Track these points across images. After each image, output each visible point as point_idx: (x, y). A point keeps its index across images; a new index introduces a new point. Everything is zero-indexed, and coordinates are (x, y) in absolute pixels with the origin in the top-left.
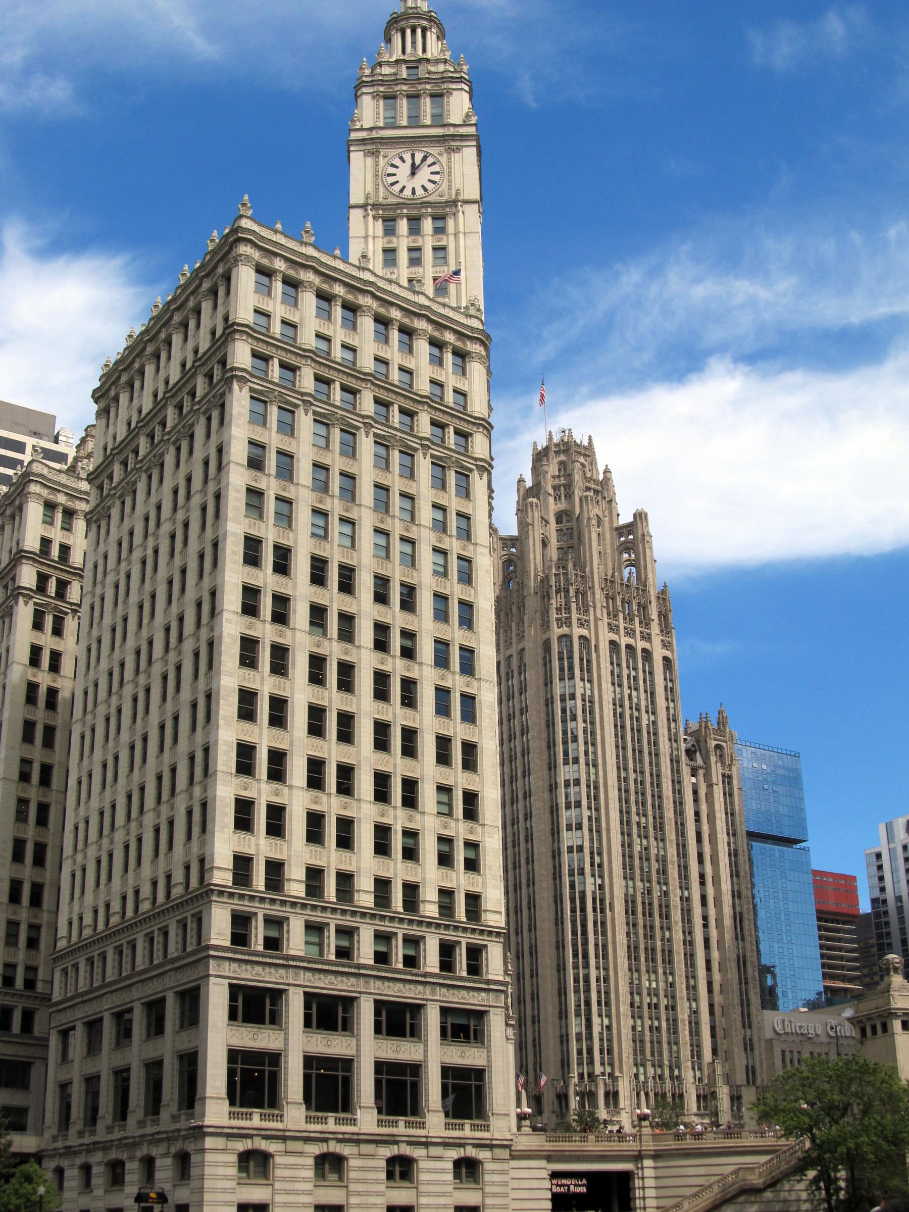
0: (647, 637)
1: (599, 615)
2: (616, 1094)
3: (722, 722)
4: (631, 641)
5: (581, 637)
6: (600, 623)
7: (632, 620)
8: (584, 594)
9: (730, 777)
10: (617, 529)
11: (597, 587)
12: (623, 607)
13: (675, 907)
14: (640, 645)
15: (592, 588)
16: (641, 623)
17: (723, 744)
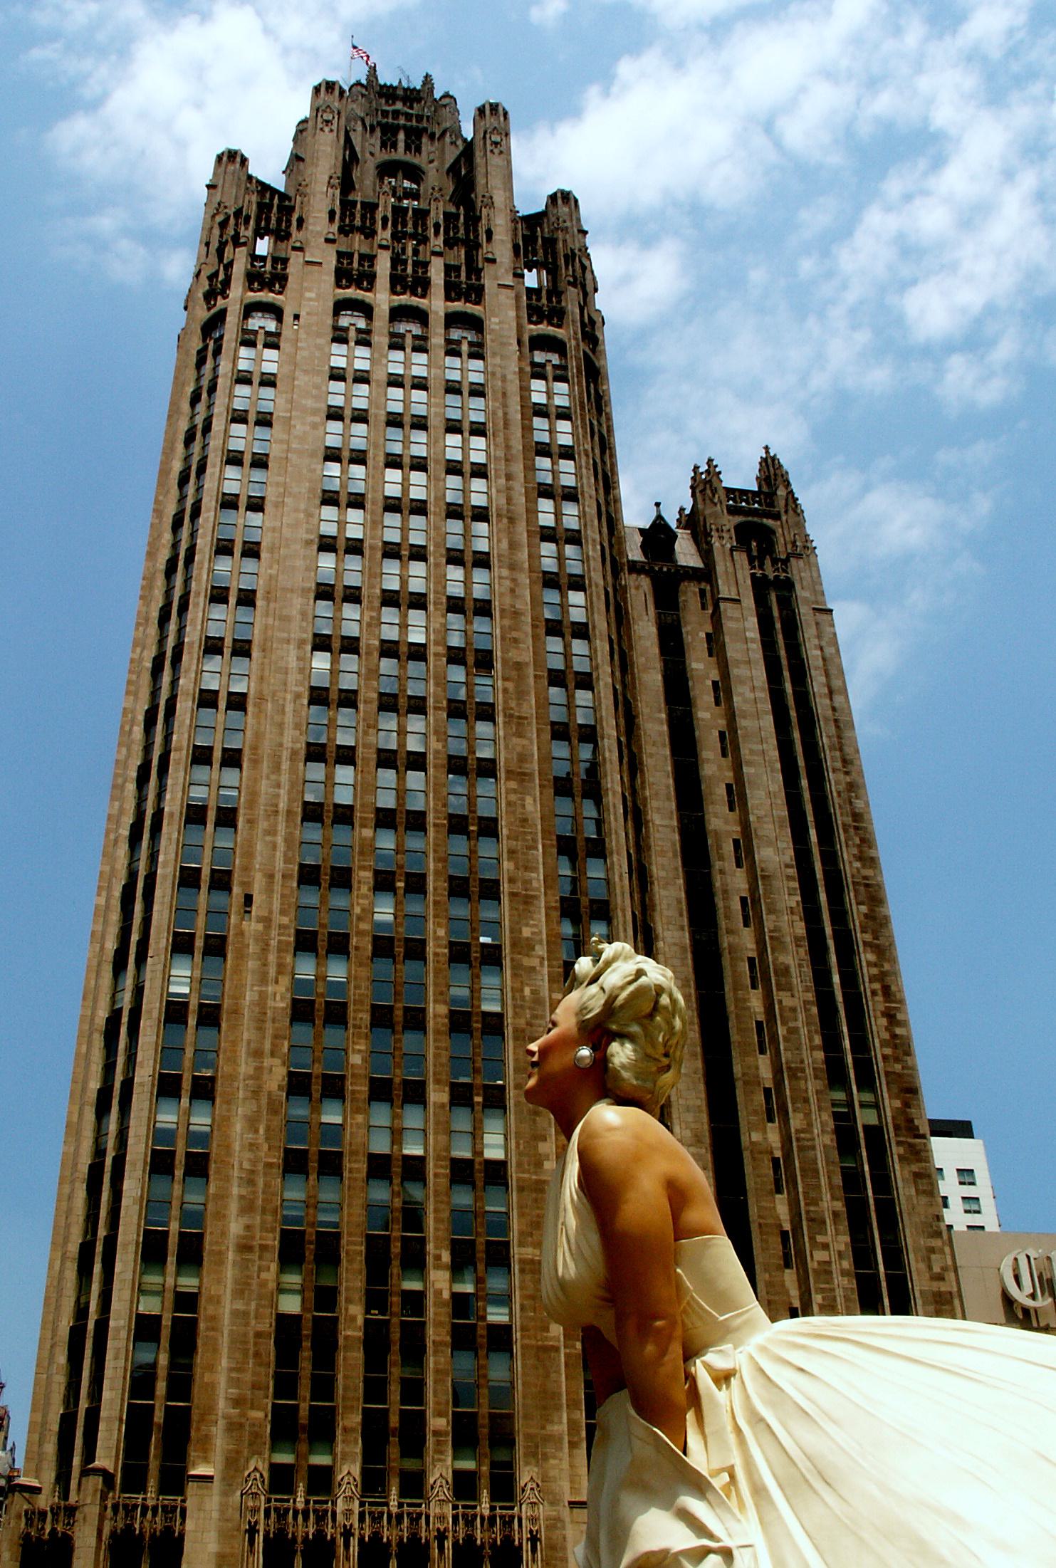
9: (786, 587)
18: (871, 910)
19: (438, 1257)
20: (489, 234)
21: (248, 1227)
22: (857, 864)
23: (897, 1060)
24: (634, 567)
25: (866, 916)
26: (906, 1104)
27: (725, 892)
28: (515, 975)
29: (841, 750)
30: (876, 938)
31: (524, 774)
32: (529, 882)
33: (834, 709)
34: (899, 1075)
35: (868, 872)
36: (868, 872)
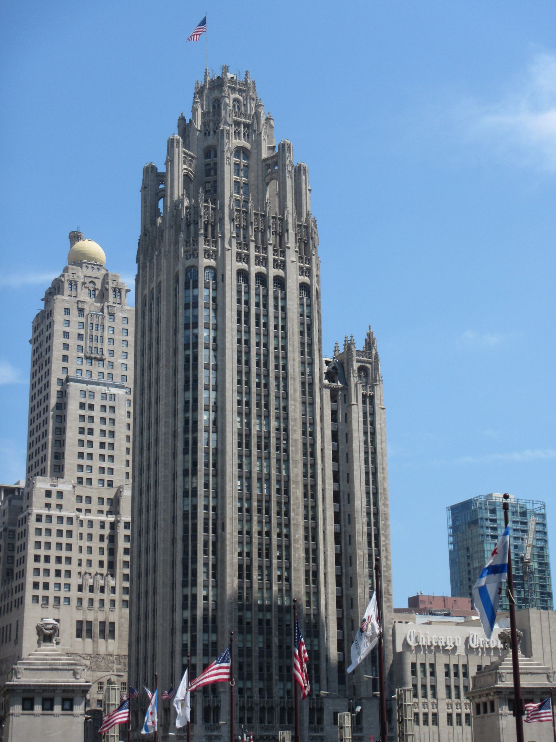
0: (282, 265)
1: (227, 246)
2: (217, 709)
3: (370, 344)
4: (263, 269)
5: (208, 267)
6: (228, 253)
7: (265, 249)
8: (213, 227)
9: (372, 398)
10: (265, 160)
11: (227, 218)
12: (256, 236)
13: (297, 525)
14: (273, 272)
15: (222, 220)
16: (275, 251)
17: (369, 366)
18: (385, 522)
19: (275, 634)
20: (287, 231)
21: (231, 626)
22: (383, 507)
23: (387, 571)
24: (326, 387)
25: (383, 525)
26: (388, 585)
27: (344, 512)
28: (294, 550)
29: (382, 464)
30: (385, 532)
31: (296, 482)
32: (297, 520)
33: (382, 449)
34: (387, 576)
35: (385, 509)
36: (385, 509)
